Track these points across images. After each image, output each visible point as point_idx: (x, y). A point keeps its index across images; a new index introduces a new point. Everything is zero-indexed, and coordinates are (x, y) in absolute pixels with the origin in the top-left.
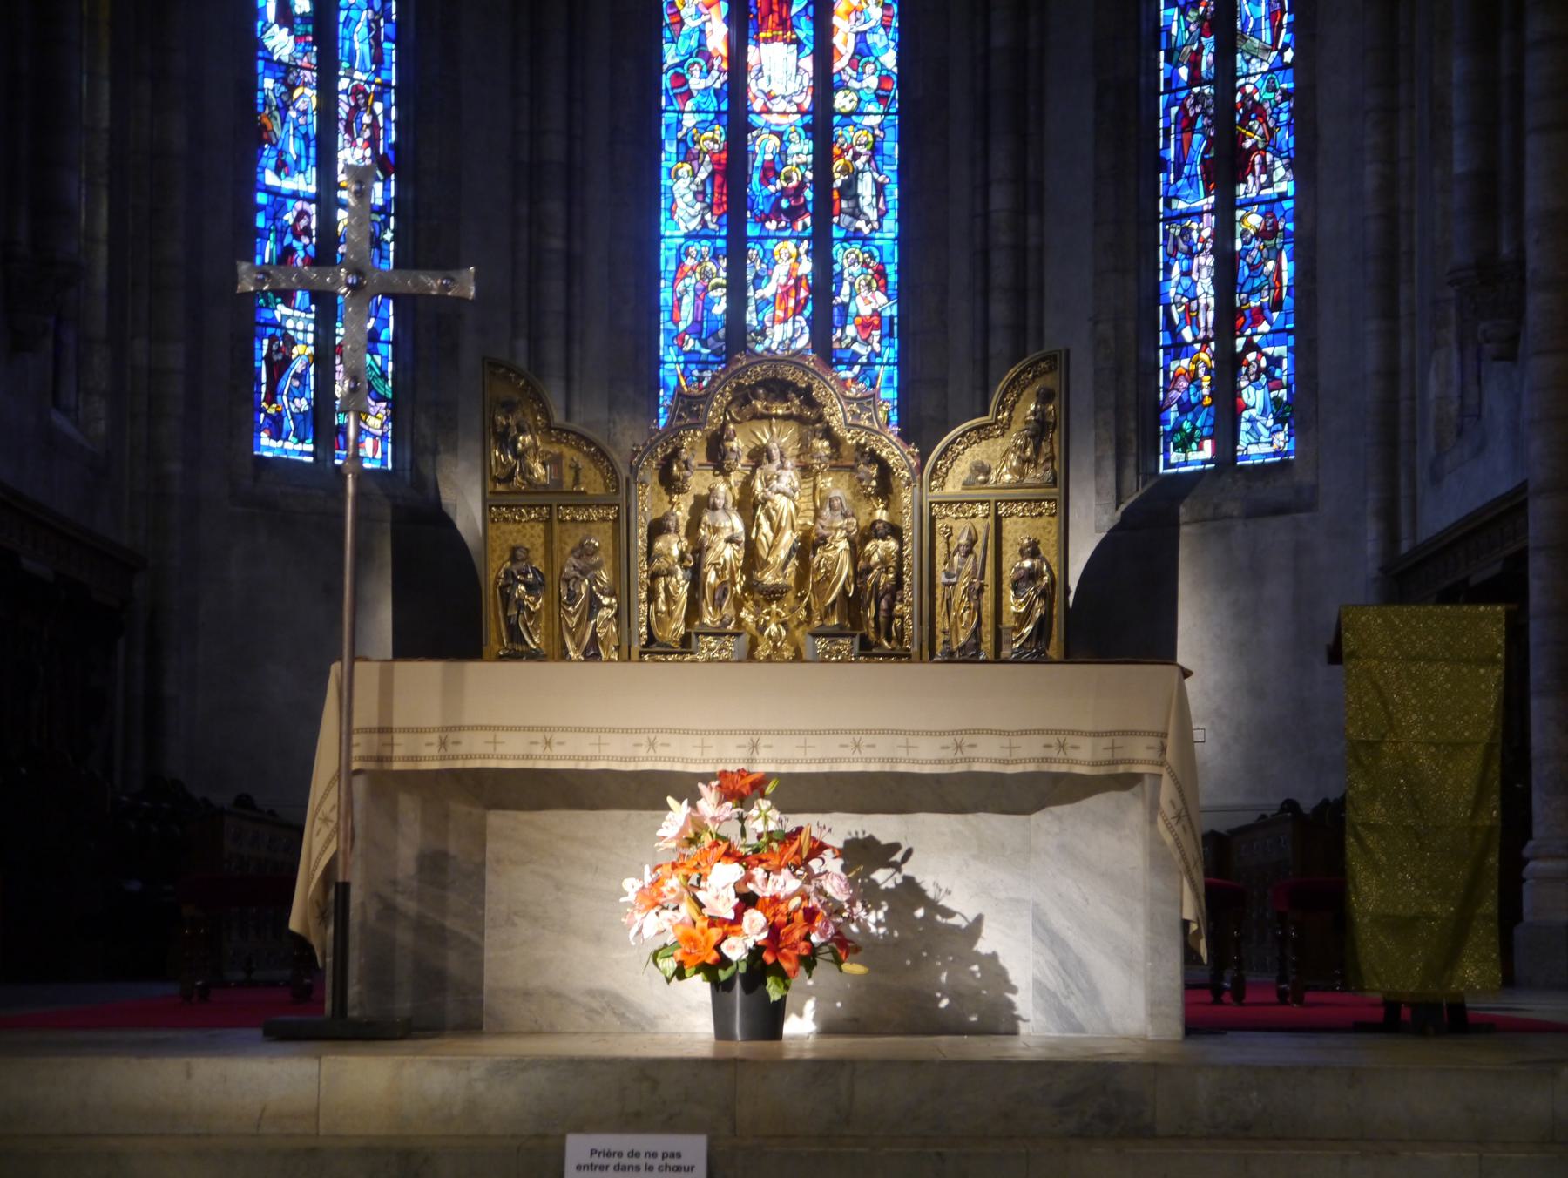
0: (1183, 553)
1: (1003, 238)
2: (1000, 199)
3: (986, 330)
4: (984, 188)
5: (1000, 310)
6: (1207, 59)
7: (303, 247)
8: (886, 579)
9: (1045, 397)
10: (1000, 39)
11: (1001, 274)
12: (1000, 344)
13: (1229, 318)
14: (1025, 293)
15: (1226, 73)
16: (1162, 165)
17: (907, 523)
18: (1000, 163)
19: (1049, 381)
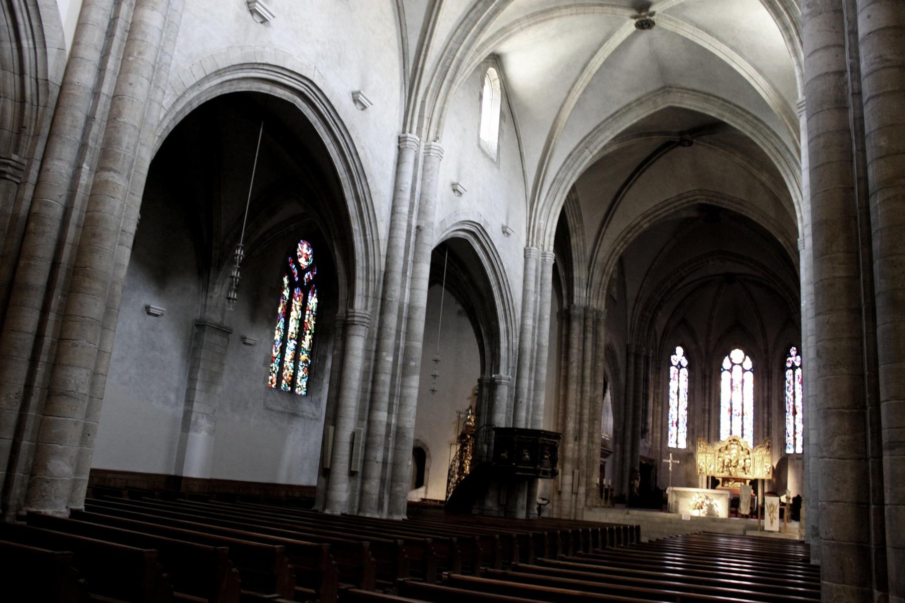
0: (789, 463)
1: (766, 420)
2: (766, 416)
3: (764, 433)
4: (764, 414)
5: (766, 430)
6: (792, 399)
7: (675, 421)
8: (749, 465)
9: (769, 443)
10: (766, 395)
11: (766, 423)
12: (766, 434)
13: (795, 433)
14: (769, 428)
15: (794, 401)
16: (786, 412)
17: (751, 458)
18: (766, 410)
19: (769, 441)
